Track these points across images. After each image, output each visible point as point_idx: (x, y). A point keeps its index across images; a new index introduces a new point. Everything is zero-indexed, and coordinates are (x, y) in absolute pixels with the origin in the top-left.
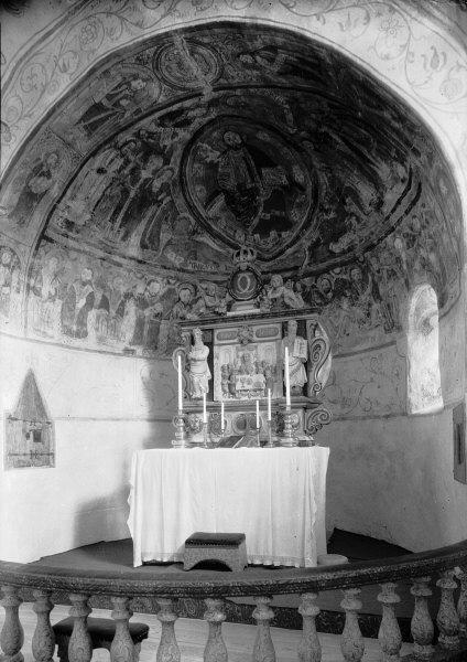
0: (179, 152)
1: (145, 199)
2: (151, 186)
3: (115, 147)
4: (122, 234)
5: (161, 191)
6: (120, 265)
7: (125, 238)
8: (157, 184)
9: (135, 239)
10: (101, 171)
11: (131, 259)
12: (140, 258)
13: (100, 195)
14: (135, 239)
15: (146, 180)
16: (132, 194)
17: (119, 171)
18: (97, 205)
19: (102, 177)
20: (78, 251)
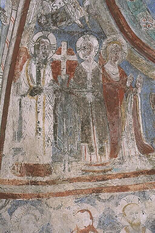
0: (106, 16)
1: (112, 97)
2: (106, 76)
3: (29, 57)
4: (108, 150)
5: (123, 74)
6: (123, 189)
7: (115, 149)
8: (112, 70)
9: (129, 147)
10: (34, 92)
11: (137, 174)
12: (149, 168)
13: (52, 119)
14: (129, 147)
15: (96, 73)
16: (90, 97)
17: (55, 80)
18: (55, 132)
19: (41, 97)
20: (60, 194)
